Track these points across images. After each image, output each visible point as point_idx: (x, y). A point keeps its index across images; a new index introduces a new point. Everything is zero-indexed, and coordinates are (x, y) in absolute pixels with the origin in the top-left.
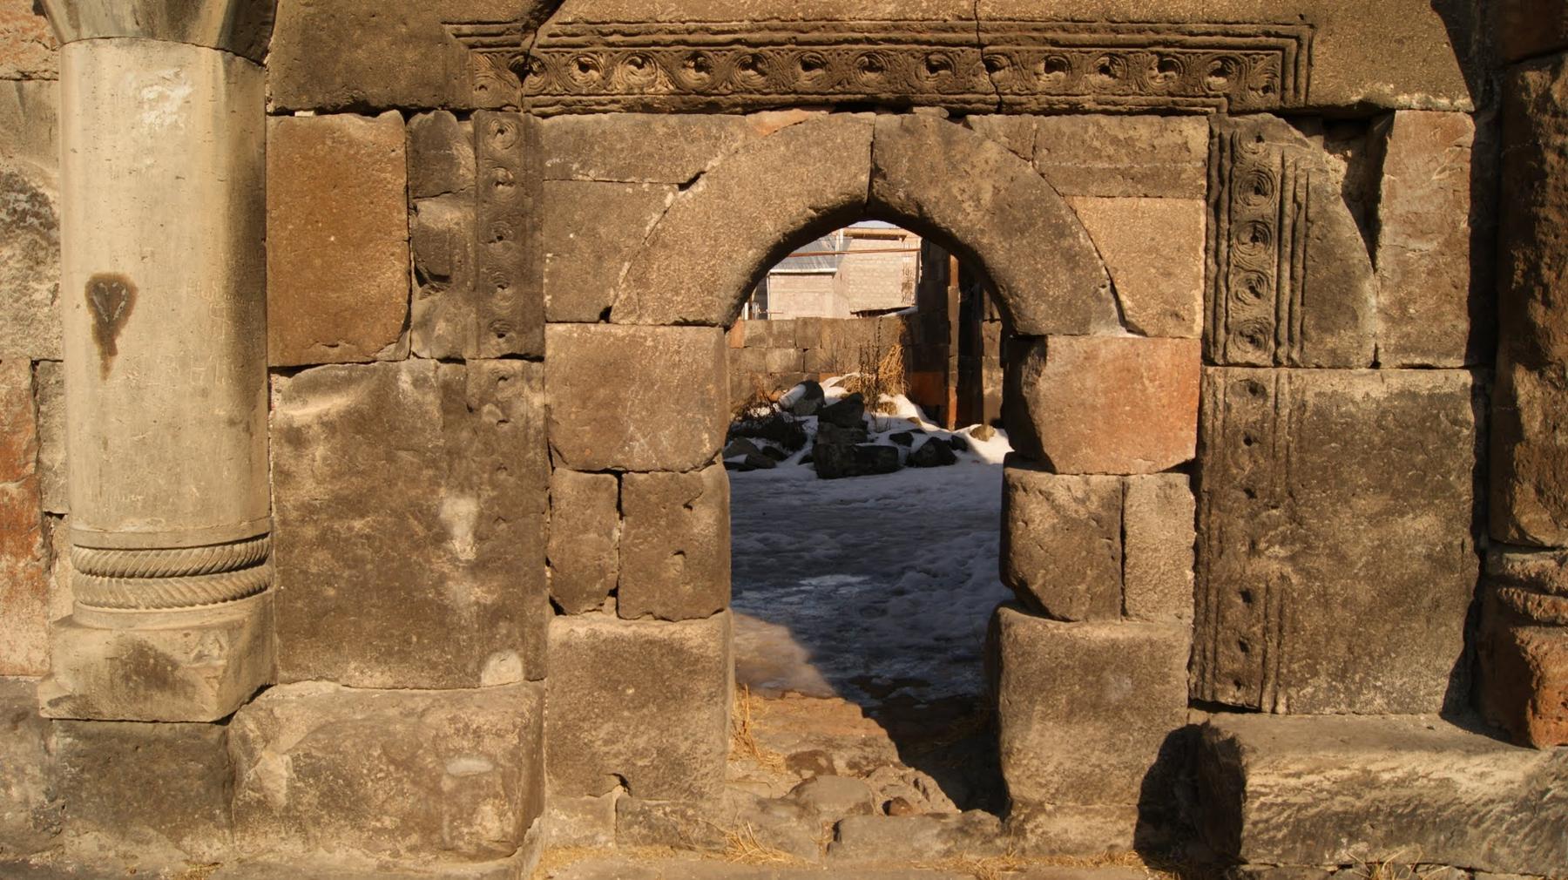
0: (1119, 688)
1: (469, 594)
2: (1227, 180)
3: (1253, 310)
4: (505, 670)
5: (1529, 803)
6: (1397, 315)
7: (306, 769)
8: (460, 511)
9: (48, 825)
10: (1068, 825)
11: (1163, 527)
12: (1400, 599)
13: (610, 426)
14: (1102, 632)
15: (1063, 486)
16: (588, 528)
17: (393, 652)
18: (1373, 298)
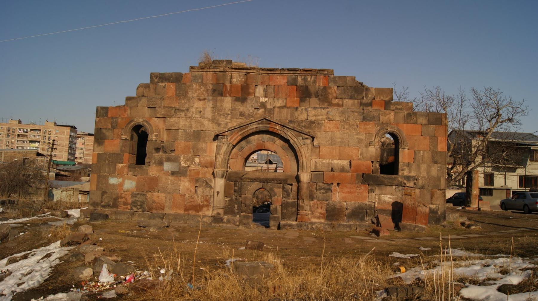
0: (276, 219)
1: (236, 211)
2: (283, 188)
3: (284, 196)
4: (238, 216)
5: (297, 225)
6: (293, 196)
7: (227, 220)
8: (236, 206)
9: (211, 223)
10: (273, 228)
11: (279, 208)
12: (293, 214)
13: (246, 201)
14: (275, 215)
15: (273, 206)
16: (244, 208)
17: (231, 214)
18: (291, 195)
